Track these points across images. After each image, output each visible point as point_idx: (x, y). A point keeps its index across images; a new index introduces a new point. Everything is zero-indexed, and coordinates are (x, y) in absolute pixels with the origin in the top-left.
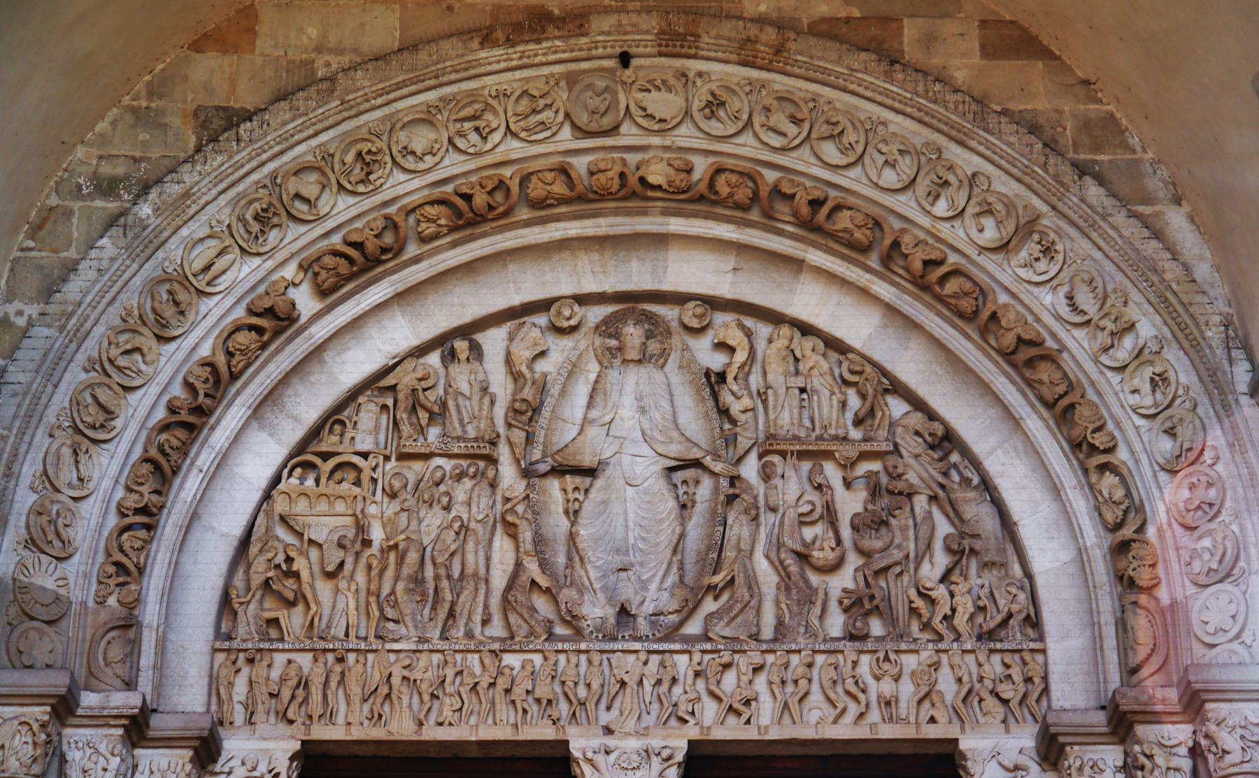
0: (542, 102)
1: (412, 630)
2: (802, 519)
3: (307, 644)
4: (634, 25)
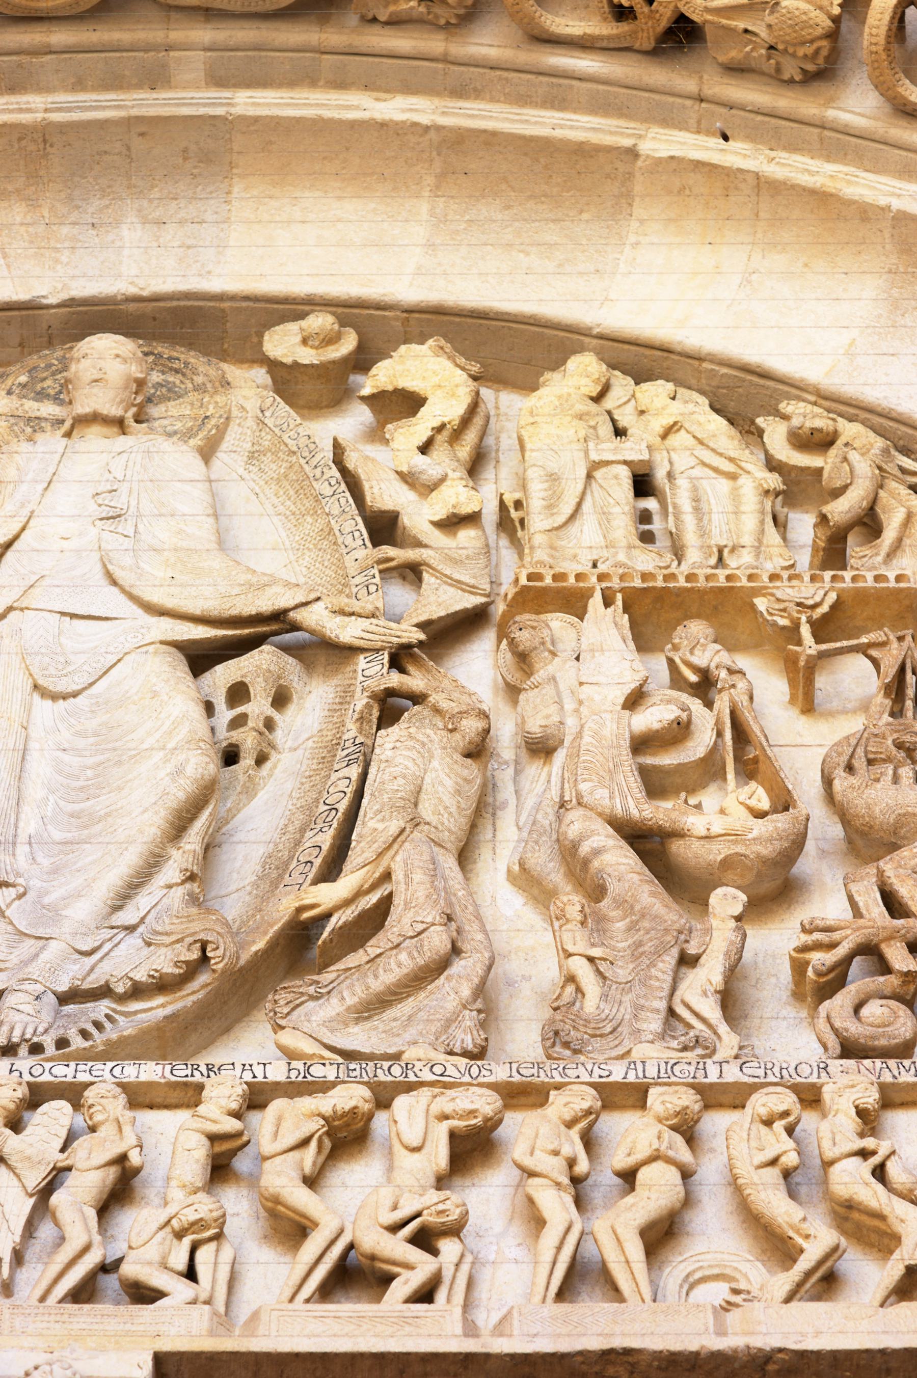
2: (649, 760)
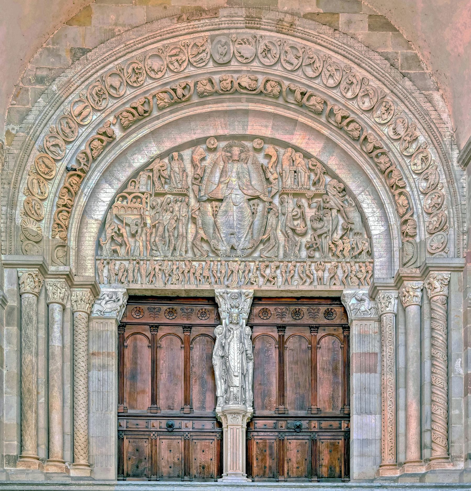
0: (202, 49)
1: (161, 253)
3: (127, 257)
4: (236, 13)
